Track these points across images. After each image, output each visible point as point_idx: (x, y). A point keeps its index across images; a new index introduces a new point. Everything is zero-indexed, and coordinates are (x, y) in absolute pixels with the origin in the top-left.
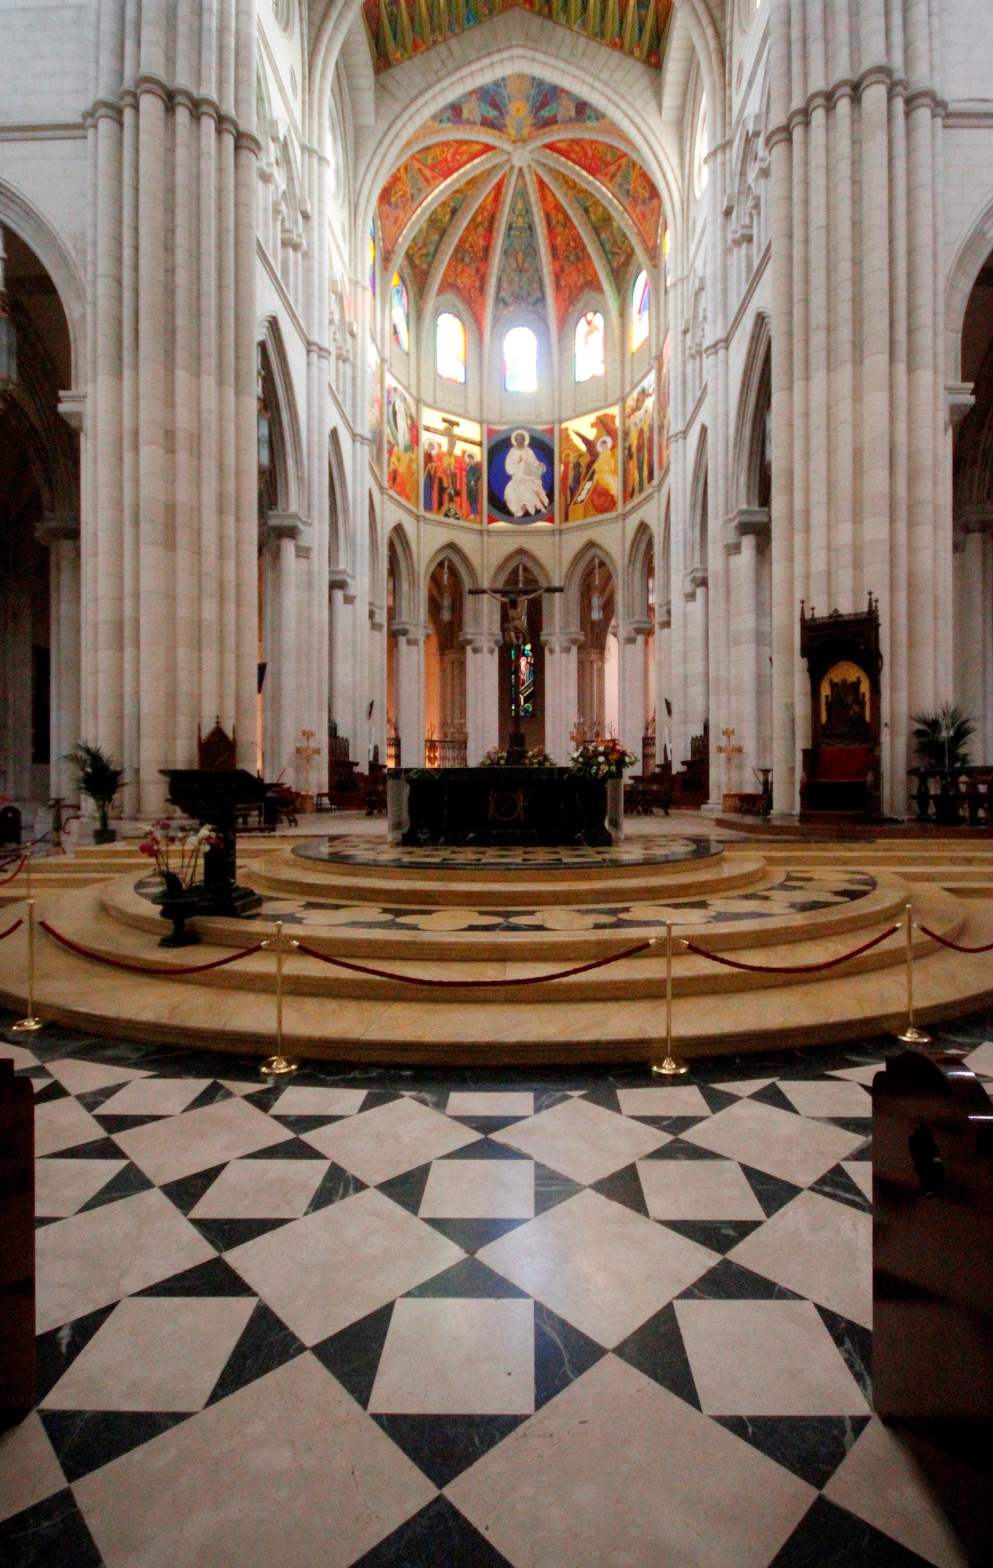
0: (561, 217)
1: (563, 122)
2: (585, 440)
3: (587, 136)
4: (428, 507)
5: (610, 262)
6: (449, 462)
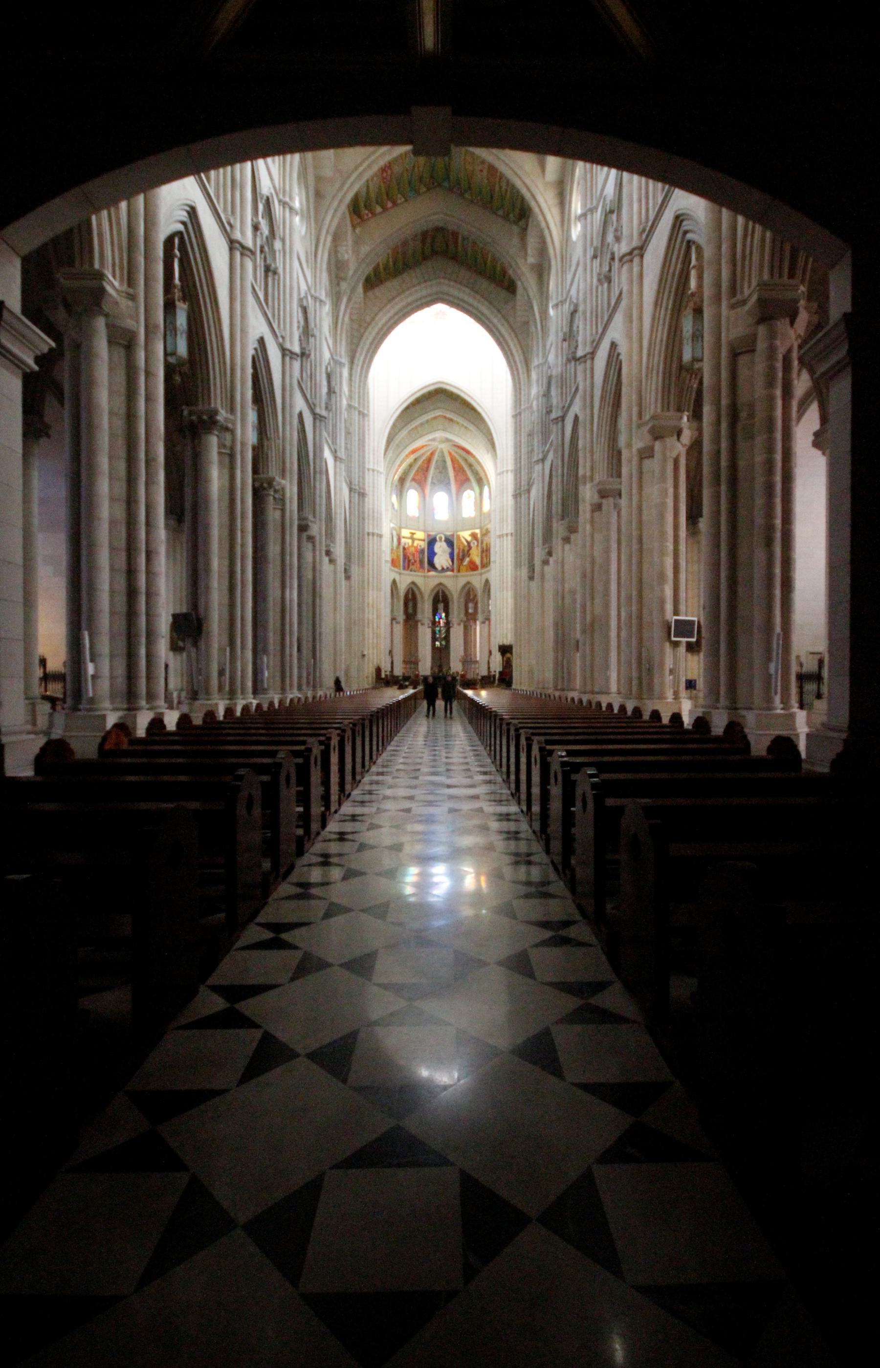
2: (467, 541)
4: (404, 569)
6: (412, 550)
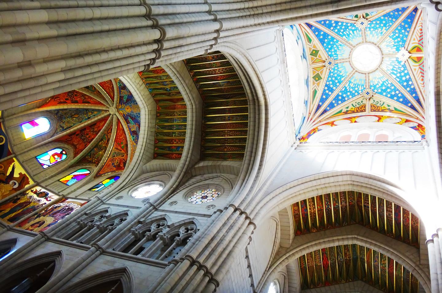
0: (96, 129)
1: (128, 126)
3: (128, 136)
5: (87, 155)
